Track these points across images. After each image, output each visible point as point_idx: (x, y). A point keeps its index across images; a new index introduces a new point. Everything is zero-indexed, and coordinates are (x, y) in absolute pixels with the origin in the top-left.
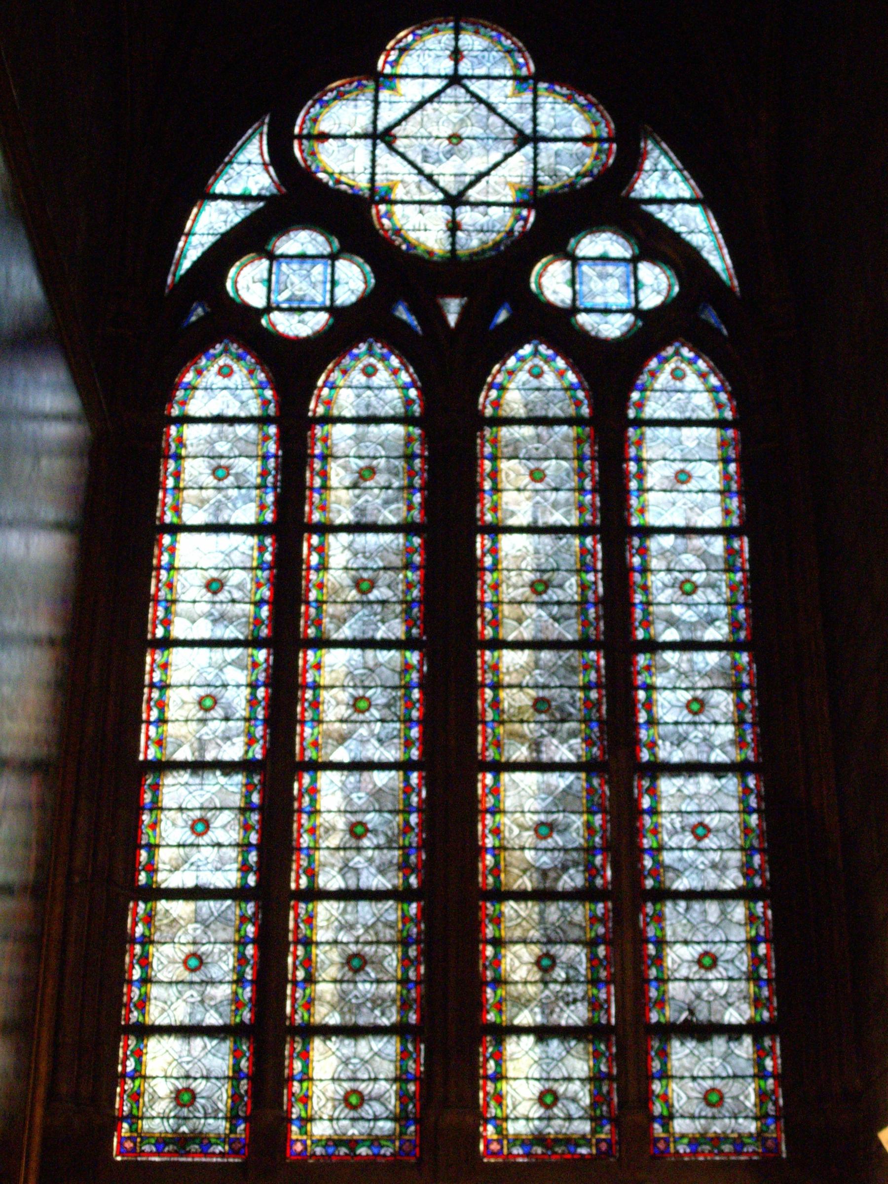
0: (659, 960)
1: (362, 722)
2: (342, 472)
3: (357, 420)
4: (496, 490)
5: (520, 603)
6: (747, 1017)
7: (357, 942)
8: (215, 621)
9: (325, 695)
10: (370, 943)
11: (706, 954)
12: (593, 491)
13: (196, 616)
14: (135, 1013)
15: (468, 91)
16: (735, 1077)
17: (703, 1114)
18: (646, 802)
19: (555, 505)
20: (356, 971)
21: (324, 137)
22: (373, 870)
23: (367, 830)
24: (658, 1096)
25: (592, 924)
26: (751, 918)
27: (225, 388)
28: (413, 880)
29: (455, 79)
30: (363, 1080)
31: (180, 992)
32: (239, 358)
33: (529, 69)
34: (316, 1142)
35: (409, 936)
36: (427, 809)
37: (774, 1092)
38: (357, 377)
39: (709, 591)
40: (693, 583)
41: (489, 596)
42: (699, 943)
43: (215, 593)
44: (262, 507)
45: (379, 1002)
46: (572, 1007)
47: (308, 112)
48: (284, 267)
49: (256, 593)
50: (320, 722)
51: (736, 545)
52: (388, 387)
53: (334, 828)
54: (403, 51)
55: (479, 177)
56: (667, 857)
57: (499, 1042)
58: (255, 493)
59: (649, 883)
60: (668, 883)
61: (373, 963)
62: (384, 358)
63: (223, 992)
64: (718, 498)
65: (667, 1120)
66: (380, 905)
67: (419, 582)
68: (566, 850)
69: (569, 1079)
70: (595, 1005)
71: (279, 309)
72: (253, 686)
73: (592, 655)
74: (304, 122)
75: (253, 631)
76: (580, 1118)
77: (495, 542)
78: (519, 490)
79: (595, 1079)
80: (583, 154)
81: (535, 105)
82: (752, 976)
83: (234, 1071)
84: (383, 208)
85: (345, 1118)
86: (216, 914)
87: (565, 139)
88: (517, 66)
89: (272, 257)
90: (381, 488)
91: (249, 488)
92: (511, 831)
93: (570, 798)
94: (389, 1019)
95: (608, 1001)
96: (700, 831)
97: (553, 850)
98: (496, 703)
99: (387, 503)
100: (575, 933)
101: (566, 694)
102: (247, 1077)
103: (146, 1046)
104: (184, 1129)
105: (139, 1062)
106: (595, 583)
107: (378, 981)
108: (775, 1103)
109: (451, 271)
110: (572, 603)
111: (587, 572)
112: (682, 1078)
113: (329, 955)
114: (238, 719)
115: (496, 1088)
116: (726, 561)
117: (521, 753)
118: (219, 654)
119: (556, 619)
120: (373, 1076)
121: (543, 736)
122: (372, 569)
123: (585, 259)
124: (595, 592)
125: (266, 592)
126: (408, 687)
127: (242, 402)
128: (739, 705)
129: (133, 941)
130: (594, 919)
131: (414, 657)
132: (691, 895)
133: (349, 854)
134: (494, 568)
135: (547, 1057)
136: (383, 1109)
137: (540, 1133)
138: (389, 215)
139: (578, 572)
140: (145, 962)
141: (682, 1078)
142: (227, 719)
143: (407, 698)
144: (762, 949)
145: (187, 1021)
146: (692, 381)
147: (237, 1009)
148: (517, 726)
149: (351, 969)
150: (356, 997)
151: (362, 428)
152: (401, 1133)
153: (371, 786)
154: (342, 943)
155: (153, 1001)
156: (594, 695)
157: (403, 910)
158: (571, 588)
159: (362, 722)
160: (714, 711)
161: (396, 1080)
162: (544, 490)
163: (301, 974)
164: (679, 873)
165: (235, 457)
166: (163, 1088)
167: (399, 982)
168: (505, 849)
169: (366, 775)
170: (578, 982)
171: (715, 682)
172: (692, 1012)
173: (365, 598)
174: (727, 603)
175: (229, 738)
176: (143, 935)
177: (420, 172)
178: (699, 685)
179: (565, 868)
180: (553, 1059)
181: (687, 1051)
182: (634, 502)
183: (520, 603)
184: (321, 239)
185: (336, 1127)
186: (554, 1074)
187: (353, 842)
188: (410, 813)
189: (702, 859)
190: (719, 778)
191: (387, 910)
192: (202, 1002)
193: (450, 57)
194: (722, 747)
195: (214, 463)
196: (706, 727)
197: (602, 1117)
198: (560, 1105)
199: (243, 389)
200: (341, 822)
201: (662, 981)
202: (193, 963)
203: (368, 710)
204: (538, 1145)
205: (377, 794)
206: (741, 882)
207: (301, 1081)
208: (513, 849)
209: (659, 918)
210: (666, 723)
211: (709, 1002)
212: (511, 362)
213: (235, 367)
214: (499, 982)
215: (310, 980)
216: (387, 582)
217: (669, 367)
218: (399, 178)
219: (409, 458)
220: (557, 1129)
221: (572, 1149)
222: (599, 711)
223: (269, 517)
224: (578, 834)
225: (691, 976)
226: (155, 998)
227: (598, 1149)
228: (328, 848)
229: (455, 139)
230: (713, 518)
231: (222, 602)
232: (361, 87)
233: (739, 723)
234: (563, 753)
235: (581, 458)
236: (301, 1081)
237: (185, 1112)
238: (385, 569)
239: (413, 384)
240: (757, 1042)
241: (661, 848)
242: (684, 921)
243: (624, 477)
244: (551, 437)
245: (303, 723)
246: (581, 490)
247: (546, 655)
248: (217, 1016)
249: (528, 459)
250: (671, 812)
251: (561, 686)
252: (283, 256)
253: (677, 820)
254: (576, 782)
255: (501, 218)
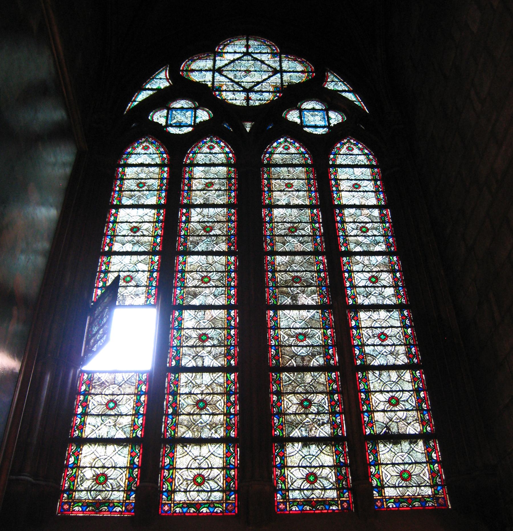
0: (367, 401)
1: (206, 287)
2: (198, 185)
3: (205, 165)
4: (270, 191)
5: (284, 236)
6: (419, 430)
7: (202, 394)
8: (134, 244)
9: (187, 275)
10: (209, 394)
11: (392, 397)
12: (315, 191)
13: (125, 242)
14: (77, 432)
15: (252, 57)
16: (416, 463)
17: (401, 485)
18: (353, 323)
19: (298, 197)
20: (201, 409)
21: (193, 71)
22: (211, 357)
23: (208, 338)
24: (374, 475)
25: (330, 384)
26: (414, 379)
27: (145, 154)
28: (233, 362)
29: (247, 54)
30: (205, 469)
31: (103, 421)
32: (152, 143)
33: (277, 50)
34: (177, 504)
35: (230, 390)
36: (241, 328)
37: (439, 471)
38: (205, 150)
39: (374, 231)
40: (367, 228)
41: (268, 233)
42: (388, 392)
43: (135, 232)
44: (159, 198)
45: (214, 425)
46: (322, 427)
47: (186, 63)
48: (174, 112)
49: (155, 232)
50: (186, 287)
51: (385, 212)
52: (221, 153)
53: (191, 337)
54: (225, 46)
55: (258, 83)
56: (368, 349)
57: (283, 447)
58: (156, 192)
59: (359, 362)
60: (368, 362)
61: (210, 404)
62: (217, 143)
63: (126, 421)
64: (374, 194)
65: (381, 488)
66: (214, 375)
67: (234, 227)
68: (312, 346)
69: (322, 466)
70: (334, 425)
71: (171, 126)
72: (151, 272)
73: (320, 258)
74: (184, 66)
75: (153, 248)
76: (330, 489)
77: (270, 212)
78: (281, 191)
79: (337, 466)
80: (302, 76)
81: (281, 61)
82: (418, 409)
83: (130, 464)
84: (217, 93)
85: (193, 491)
86: (126, 380)
87: (293, 72)
88: (272, 50)
89: (169, 109)
90: (216, 190)
91: (154, 190)
92: (284, 337)
93: (314, 322)
94: (219, 435)
95: (341, 423)
96: (382, 337)
97: (306, 346)
98: (274, 279)
99: (218, 196)
100: (321, 388)
101: (309, 275)
102: (138, 467)
103: (81, 450)
104: (99, 497)
105: (77, 459)
106: (319, 228)
107: (213, 414)
108: (441, 478)
109: (247, 112)
110: (309, 236)
111: (315, 223)
112: (387, 464)
113: (186, 400)
114: (143, 286)
115: (281, 472)
116: (381, 218)
117: (288, 301)
118: (135, 258)
119: (302, 243)
120: (210, 466)
121: (298, 293)
122: (211, 222)
123: (305, 109)
124: (320, 231)
125: (160, 232)
126: (230, 272)
127: (153, 159)
128: (395, 278)
129: (80, 394)
130: (330, 381)
131: (232, 259)
132: (381, 368)
133: (198, 349)
134: (271, 222)
135: (310, 455)
136: (216, 485)
137: (308, 498)
138: (220, 95)
139: (311, 223)
140: (85, 405)
141: (387, 464)
142: (137, 286)
143: (229, 276)
144: (422, 394)
145: (105, 436)
146: (356, 151)
147: (134, 429)
148: (285, 289)
149: (198, 408)
150: (201, 423)
151: (207, 168)
152: (226, 499)
153: (210, 317)
154: (193, 394)
155: (87, 425)
156: (322, 275)
157: (227, 377)
158: (308, 229)
159: (206, 287)
160: (382, 281)
161: (223, 468)
162: (293, 191)
163: (170, 411)
164: (374, 357)
165: (148, 179)
166: (89, 473)
167: (225, 415)
168: (282, 346)
169: (207, 311)
170: (323, 413)
171: (382, 269)
172: (388, 428)
173: (208, 234)
174: (382, 236)
175: (137, 295)
176: (85, 390)
177: (232, 81)
178: (374, 270)
179: (314, 356)
180: (313, 456)
181: (388, 450)
182: (335, 195)
183: (284, 236)
184: (190, 103)
185: (188, 496)
186: (314, 464)
187: (200, 343)
188: (230, 329)
189: (385, 350)
190: (389, 312)
191: (218, 377)
192: (115, 425)
193: (245, 47)
194: (389, 297)
195: (138, 181)
196: (380, 289)
197: (343, 488)
198: (318, 481)
199: (154, 154)
200: (194, 334)
201: (371, 412)
202: (112, 405)
203: (209, 282)
204: (308, 505)
205: (213, 320)
206: (406, 361)
207: (169, 470)
208: (285, 346)
209: (366, 380)
210: (359, 287)
211: (397, 422)
212: (275, 144)
213: (150, 146)
214: (282, 414)
215: (176, 414)
216: (219, 227)
217: (345, 147)
218: (224, 83)
219: (229, 179)
220: (318, 496)
221: (327, 507)
222: (325, 282)
223: (163, 202)
224: (319, 339)
225: (386, 409)
226: (89, 424)
227: (342, 506)
228: (187, 346)
229: (248, 71)
230: (373, 201)
231: (138, 236)
232: (208, 56)
233: (396, 287)
234: (309, 301)
235: (309, 179)
236: (169, 470)
237: (100, 487)
238: (218, 222)
239: (231, 152)
240: (426, 444)
241: (363, 345)
242: (379, 381)
243: (330, 186)
244: (295, 171)
245: (176, 287)
246: (310, 191)
247: (298, 258)
248: (123, 433)
249: (285, 179)
250: (367, 328)
251: (306, 271)
252: (174, 108)
253: (370, 332)
254: (316, 314)
255: (268, 97)
